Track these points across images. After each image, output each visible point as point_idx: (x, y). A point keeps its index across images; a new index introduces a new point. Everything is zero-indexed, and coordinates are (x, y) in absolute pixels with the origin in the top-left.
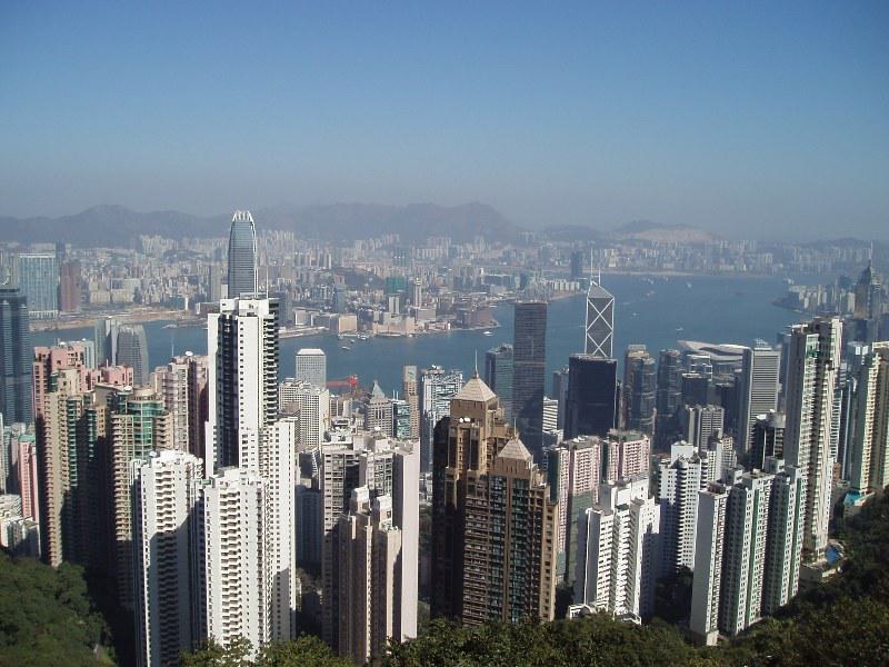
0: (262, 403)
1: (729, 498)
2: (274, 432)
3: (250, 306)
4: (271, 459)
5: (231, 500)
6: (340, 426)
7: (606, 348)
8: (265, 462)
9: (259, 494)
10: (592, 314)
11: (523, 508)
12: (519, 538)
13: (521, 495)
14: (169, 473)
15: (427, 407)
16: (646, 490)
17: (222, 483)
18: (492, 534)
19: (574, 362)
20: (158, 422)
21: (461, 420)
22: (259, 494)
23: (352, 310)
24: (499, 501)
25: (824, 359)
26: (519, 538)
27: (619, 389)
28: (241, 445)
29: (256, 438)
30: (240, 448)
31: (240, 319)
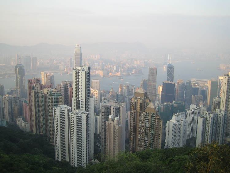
3: (83, 68)
5: (79, 118)
7: (172, 80)
8: (87, 108)
9: (86, 116)
11: (154, 121)
14: (63, 111)
15: (126, 94)
17: (77, 113)
19: (163, 83)
20: (60, 98)
24: (147, 118)
27: (175, 91)
30: (81, 105)
31: (81, 72)
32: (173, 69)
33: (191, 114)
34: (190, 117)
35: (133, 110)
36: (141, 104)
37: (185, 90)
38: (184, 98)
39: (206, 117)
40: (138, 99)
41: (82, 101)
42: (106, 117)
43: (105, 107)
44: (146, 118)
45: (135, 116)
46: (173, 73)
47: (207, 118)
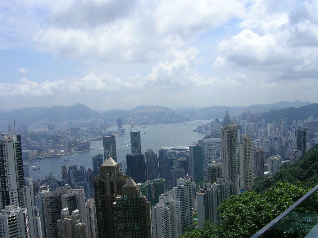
0: (18, 179)
1: (207, 194)
2: (23, 191)
4: (24, 202)
6: (44, 190)
8: (21, 204)
10: (132, 139)
11: (137, 206)
12: (136, 219)
13: (135, 201)
15: (72, 181)
16: (175, 196)
17: (7, 213)
18: (125, 218)
21: (105, 175)
22: (24, 215)
23: (34, 148)
24: (126, 204)
25: (233, 139)
26: (136, 219)
27: (146, 165)
28: (11, 198)
29: (17, 193)
31: (6, 144)
32: (139, 136)
33: (179, 193)
34: (180, 196)
35: (99, 195)
36: (112, 184)
37: (159, 164)
38: (159, 175)
39: (207, 192)
40: (105, 177)
41: (12, 193)
42: (57, 213)
43: (51, 198)
44: (124, 203)
45: (103, 203)
46: (140, 140)
47: (209, 193)
